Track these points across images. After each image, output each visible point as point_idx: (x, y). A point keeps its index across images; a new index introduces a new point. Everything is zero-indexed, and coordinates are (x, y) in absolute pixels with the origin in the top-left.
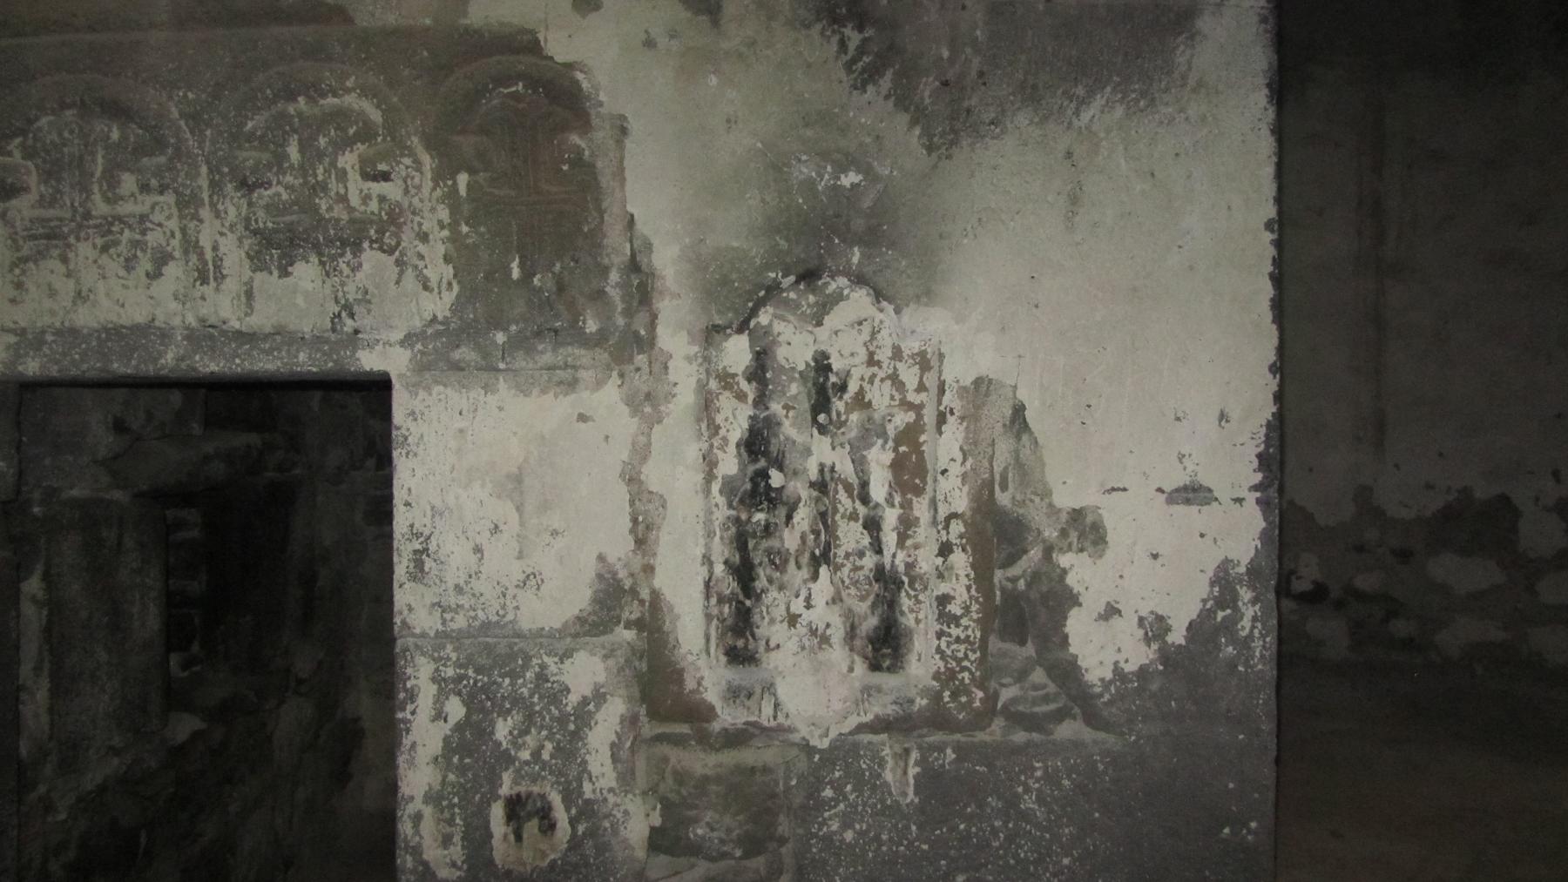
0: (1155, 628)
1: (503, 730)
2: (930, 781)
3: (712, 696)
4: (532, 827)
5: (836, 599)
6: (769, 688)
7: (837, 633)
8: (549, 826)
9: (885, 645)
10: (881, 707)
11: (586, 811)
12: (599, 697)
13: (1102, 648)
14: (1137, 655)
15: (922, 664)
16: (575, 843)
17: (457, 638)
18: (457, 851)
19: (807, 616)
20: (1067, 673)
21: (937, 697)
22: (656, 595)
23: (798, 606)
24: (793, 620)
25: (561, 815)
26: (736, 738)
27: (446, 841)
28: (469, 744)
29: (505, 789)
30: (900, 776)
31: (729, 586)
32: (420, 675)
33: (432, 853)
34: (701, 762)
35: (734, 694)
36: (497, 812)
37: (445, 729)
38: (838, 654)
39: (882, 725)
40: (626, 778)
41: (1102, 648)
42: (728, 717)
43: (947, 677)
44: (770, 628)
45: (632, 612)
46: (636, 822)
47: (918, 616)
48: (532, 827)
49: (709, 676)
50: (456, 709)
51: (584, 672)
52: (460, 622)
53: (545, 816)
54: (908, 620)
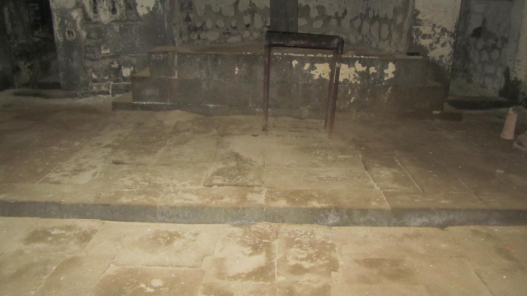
0: (148, 8)
1: (66, 22)
2: (120, 29)
3: (92, 17)
4: (71, 35)
5: (107, 4)
6: (99, 16)
7: (107, 9)
8: (73, 34)
9: (114, 11)
10: (112, 19)
11: (78, 33)
12: (77, 17)
13: (142, 11)
14: (146, 12)
15: (118, 13)
16: (76, 37)
17: (59, 10)
18: (62, 38)
19: (103, 7)
20: (137, 14)
21: (120, 18)
22: (83, 4)
23: (102, 5)
24: (101, 7)
25: (74, 33)
26: (96, 23)
27: (61, 36)
28: (62, 23)
29: (67, 29)
30: (117, 28)
31: (93, 3)
32: (55, 15)
33: (59, 38)
34: (92, 26)
35: (95, 17)
36: (66, 33)
37: (59, 22)
38: (108, 12)
39: (114, 21)
40: (82, 29)
41: (142, 11)
42: (94, 20)
43: (121, 15)
44: (99, 9)
45: (80, 6)
46: (84, 34)
47: (117, 7)
48: (71, 35)
49: (91, 14)
50: (60, 19)
51: (75, 14)
52: (59, 8)
53: (72, 33)
54: (117, 7)
